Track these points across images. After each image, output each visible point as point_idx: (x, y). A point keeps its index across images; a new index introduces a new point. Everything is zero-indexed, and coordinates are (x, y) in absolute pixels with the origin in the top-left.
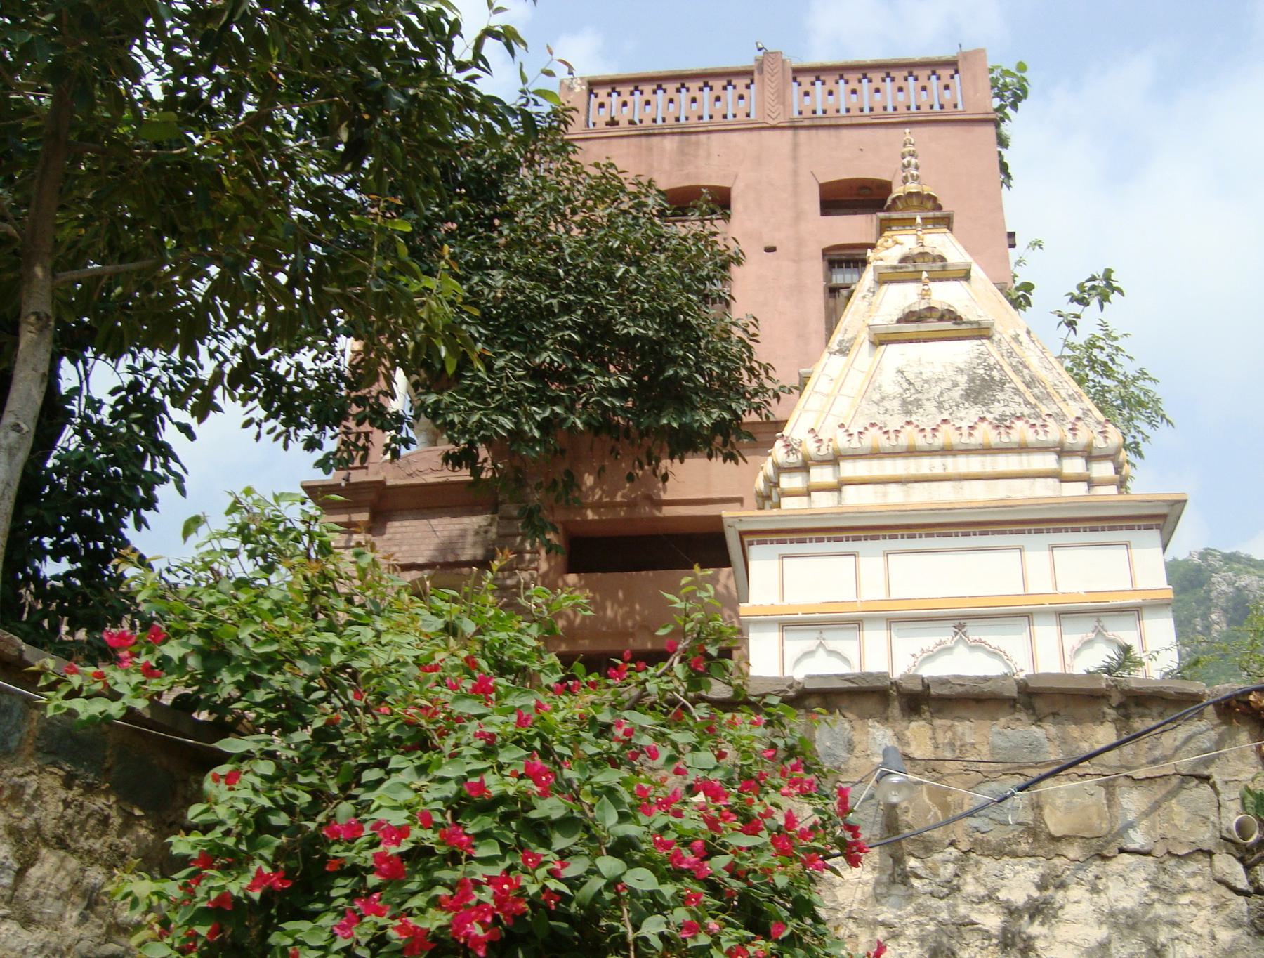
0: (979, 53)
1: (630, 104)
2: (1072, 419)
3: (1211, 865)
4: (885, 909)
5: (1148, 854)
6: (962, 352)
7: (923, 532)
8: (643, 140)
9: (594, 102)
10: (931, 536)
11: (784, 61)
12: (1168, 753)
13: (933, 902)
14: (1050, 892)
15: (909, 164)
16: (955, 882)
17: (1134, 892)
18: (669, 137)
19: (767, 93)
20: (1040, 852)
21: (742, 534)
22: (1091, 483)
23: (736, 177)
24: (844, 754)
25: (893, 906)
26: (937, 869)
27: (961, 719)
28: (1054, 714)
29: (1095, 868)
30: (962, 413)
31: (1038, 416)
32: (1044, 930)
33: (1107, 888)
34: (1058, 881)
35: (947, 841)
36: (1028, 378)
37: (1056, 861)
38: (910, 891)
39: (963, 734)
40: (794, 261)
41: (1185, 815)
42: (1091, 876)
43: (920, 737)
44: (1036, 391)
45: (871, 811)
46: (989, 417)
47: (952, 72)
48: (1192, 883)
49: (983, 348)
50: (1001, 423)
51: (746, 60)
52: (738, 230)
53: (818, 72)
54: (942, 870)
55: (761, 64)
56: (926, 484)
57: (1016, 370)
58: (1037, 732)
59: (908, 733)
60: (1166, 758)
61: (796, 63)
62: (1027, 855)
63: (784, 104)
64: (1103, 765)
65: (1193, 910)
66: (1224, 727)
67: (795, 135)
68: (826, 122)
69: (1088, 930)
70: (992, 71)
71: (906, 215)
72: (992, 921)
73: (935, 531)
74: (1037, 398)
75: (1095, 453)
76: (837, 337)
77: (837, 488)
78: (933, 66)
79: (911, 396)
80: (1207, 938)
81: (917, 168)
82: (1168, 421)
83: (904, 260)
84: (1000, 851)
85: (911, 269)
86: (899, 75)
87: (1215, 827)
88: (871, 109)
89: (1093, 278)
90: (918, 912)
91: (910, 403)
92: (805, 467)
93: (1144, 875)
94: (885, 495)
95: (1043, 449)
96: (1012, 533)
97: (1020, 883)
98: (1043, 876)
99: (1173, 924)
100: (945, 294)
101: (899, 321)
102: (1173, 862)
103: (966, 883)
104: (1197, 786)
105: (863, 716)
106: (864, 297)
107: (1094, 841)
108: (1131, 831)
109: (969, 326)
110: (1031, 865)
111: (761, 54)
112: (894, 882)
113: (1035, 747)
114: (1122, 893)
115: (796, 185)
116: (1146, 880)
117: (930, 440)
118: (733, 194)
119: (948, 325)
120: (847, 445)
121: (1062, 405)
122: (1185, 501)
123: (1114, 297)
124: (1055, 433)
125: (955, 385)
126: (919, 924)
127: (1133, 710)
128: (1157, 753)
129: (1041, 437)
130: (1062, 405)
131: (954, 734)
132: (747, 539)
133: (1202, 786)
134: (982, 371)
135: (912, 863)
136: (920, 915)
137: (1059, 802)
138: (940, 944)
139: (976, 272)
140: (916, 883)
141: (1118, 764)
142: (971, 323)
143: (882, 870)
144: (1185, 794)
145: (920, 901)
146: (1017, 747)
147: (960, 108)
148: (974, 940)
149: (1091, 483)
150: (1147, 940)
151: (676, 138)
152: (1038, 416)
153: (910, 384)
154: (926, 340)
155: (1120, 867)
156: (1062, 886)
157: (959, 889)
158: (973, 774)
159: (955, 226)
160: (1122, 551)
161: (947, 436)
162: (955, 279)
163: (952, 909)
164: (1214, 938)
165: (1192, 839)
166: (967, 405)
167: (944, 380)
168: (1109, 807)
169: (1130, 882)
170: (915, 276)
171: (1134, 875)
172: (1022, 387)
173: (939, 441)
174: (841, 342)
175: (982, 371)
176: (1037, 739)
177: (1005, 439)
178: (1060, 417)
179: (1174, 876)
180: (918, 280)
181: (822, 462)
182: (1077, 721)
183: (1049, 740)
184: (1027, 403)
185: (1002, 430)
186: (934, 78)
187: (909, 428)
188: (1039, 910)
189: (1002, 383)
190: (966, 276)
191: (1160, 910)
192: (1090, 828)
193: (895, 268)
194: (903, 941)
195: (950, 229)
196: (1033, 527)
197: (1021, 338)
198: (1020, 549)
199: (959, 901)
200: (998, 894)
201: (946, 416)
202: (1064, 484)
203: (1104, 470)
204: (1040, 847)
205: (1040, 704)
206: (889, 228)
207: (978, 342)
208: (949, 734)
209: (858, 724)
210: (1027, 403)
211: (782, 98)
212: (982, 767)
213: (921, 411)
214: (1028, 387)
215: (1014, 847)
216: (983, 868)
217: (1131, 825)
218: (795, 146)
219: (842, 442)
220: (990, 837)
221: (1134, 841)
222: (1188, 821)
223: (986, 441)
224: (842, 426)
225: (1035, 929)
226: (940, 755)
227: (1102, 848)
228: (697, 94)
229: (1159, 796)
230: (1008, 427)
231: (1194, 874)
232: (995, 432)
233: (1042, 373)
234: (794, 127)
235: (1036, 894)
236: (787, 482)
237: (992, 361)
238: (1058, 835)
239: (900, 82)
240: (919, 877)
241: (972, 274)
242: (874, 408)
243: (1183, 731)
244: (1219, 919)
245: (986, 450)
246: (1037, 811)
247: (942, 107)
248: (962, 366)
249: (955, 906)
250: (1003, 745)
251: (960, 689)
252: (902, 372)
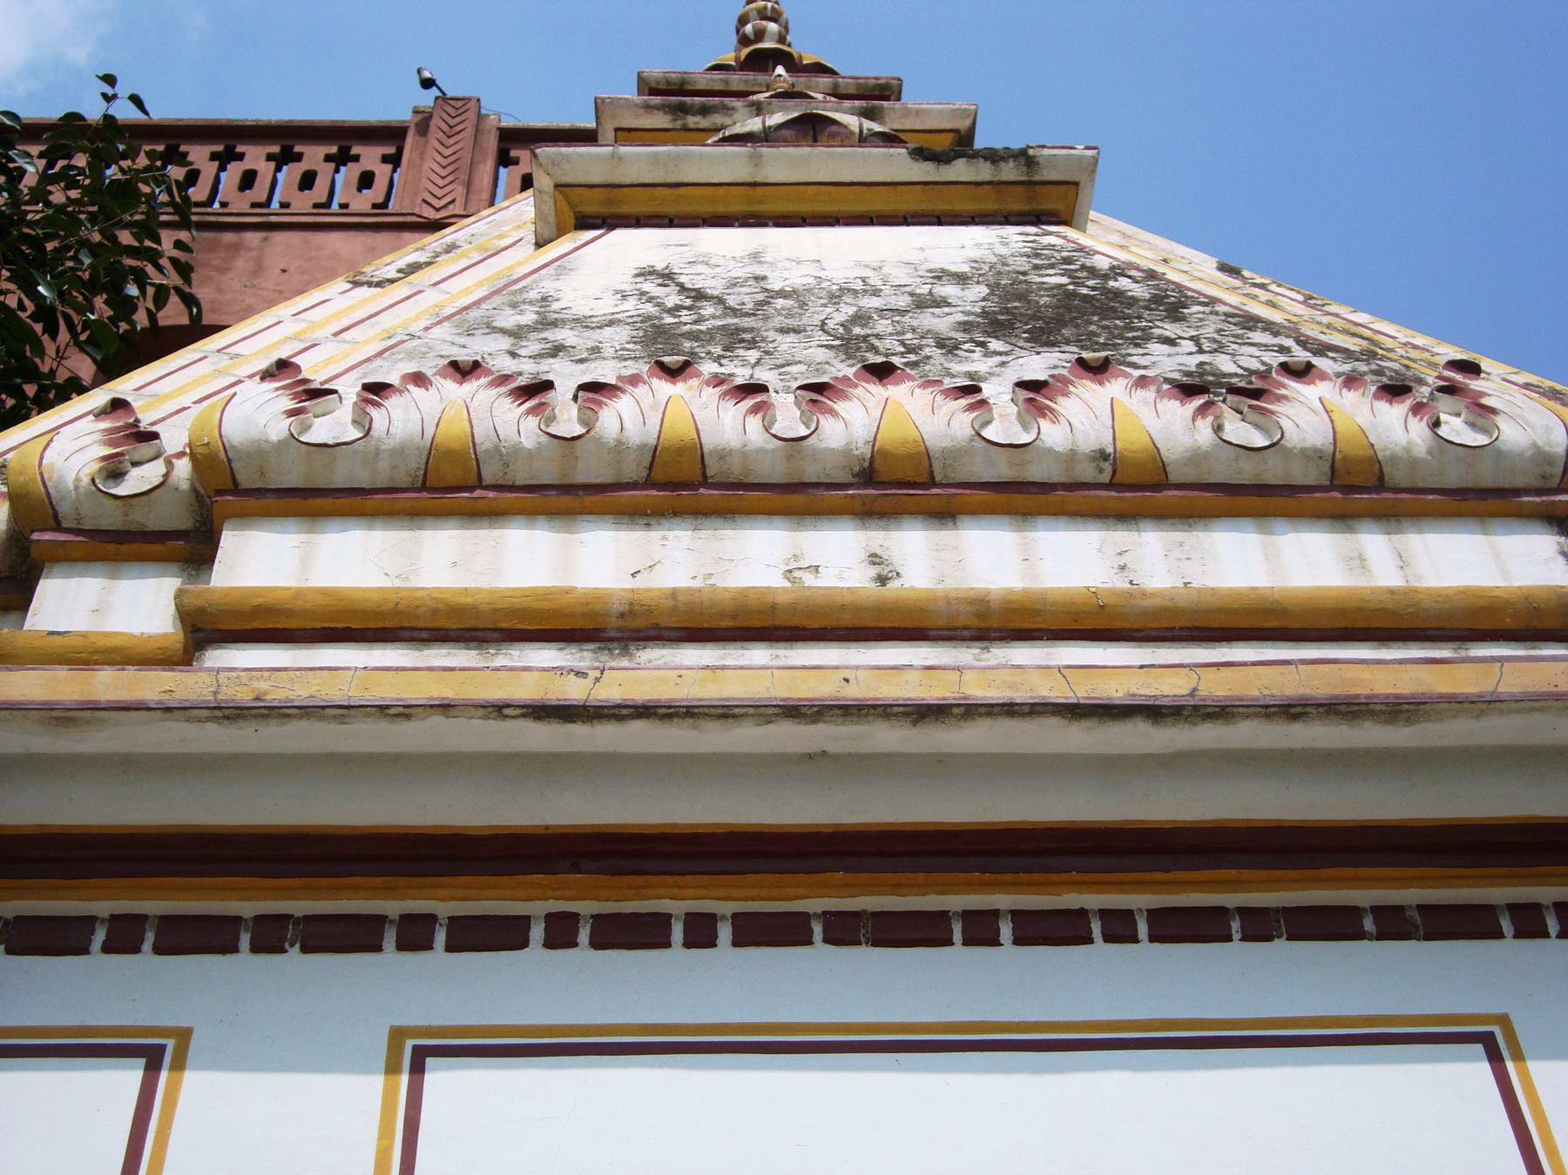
51: (396, 103)
55: (424, 121)
61: (507, 123)
109: (984, 172)
111: (427, 98)
198: (1493, 1044)
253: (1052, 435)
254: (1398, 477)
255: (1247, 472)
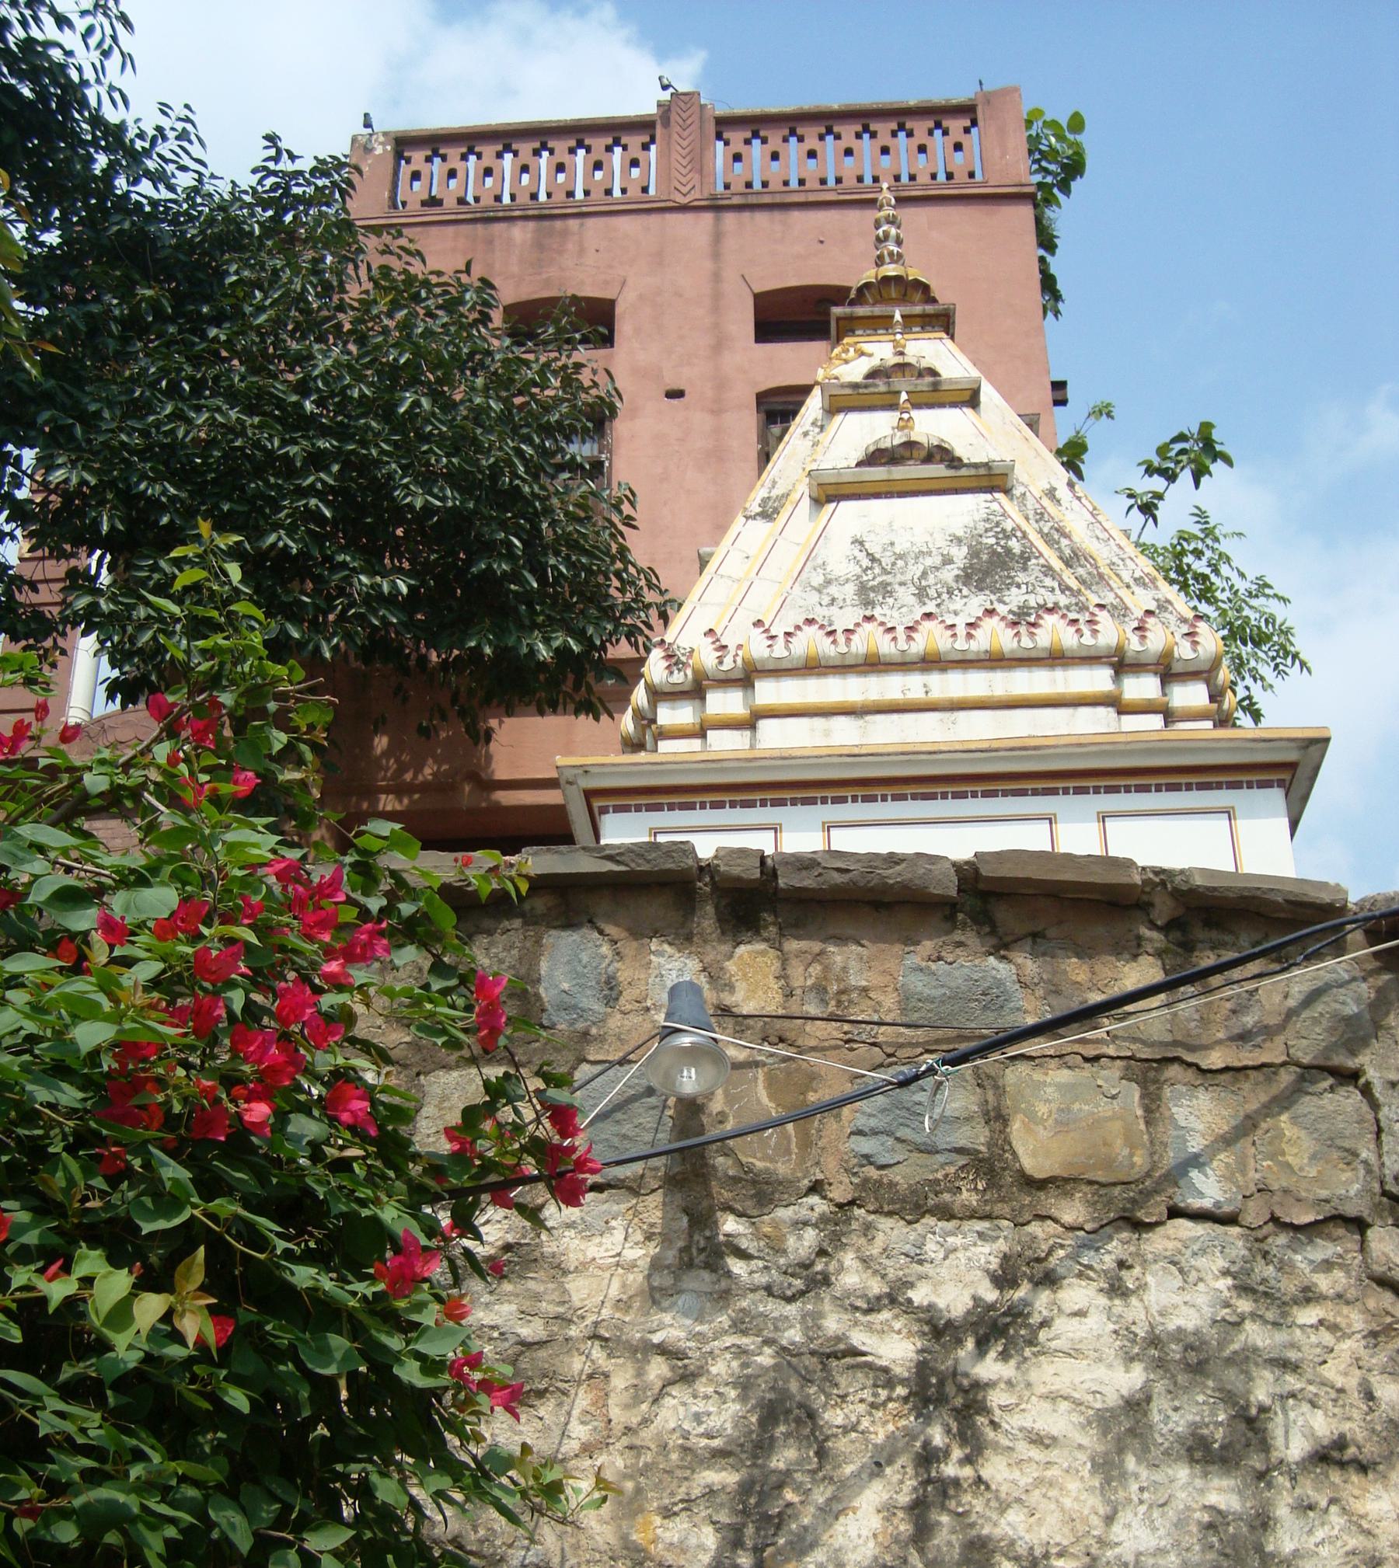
0: (1010, 93)
1: (460, 174)
2: (1139, 614)
3: (1363, 1248)
4: (667, 1318)
5: (1230, 1220)
6: (964, 511)
7: (889, 791)
8: (479, 227)
9: (405, 170)
10: (901, 797)
11: (703, 107)
12: (1273, 1021)
13: (773, 1308)
14: (1022, 1292)
15: (887, 235)
16: (819, 1267)
17: (1201, 1297)
18: (520, 224)
19: (675, 156)
20: (999, 1209)
21: (590, 794)
22: (1169, 716)
23: (624, 283)
24: (598, 1007)
25: (686, 1315)
26: (782, 1238)
27: (841, 940)
28: (1035, 936)
29: (1116, 1247)
30: (957, 603)
31: (1083, 608)
32: (1007, 1370)
33: (1143, 1287)
34: (1038, 1270)
35: (806, 1183)
36: (1067, 552)
37: (1035, 1228)
38: (724, 1284)
39: (845, 969)
40: (712, 412)
41: (1308, 1144)
42: (1109, 1262)
43: (754, 974)
44: (1081, 571)
45: (648, 1119)
46: (1002, 609)
47: (968, 123)
48: (1324, 1283)
49: (995, 506)
50: (1020, 619)
52: (628, 365)
53: (756, 125)
54: (791, 1242)
56: (895, 717)
57: (1047, 539)
58: (999, 969)
59: (731, 966)
60: (1268, 1032)
61: (721, 111)
62: (974, 1215)
63: (701, 172)
64: (1135, 1040)
65: (1327, 1338)
66: (1387, 977)
67: (717, 220)
68: (767, 199)
69: (1101, 1372)
70: (1029, 123)
71: (878, 310)
72: (896, 1348)
73: (909, 790)
74: (1083, 582)
75: (1177, 668)
76: (760, 493)
77: (749, 723)
78: (937, 114)
79: (874, 578)
80: (1355, 1397)
81: (899, 242)
82: (1303, 664)
83: (873, 374)
84: (915, 1206)
85: (882, 388)
86: (883, 128)
87: (1369, 1171)
88: (839, 180)
89: (1181, 438)
90: (739, 1326)
91: (873, 589)
92: (696, 691)
93: (1221, 1263)
94: (827, 733)
95: (1090, 659)
96: (1035, 792)
97: (957, 1271)
98: (1006, 1258)
99: (1285, 1365)
100: (933, 425)
101: (859, 464)
102: (1282, 1239)
103: (841, 1269)
104: (1332, 1089)
105: (640, 932)
106: (806, 434)
107: (1117, 1191)
108: (1194, 1174)
109: (973, 472)
110: (980, 1235)
111: (666, 96)
112: (690, 1265)
113: (993, 998)
114: (1177, 1299)
115: (717, 297)
116: (1226, 1273)
117: (902, 645)
118: (619, 310)
119: (938, 470)
120: (766, 653)
121: (1124, 593)
122: (1327, 740)
123: (1217, 467)
124: (1109, 633)
125: (948, 561)
126: (741, 1352)
127: (1199, 933)
128: (1249, 1020)
129: (1088, 640)
130: (1124, 593)
131: (826, 969)
132: (597, 804)
133: (1342, 1091)
134: (993, 541)
135: (730, 1225)
136: (744, 1333)
137: (1042, 1109)
138: (784, 1395)
139: (989, 394)
140: (737, 1266)
141: (1168, 1038)
142: (976, 466)
143: (666, 1239)
144: (1307, 1105)
145: (744, 1304)
146: (955, 997)
147: (979, 177)
148: (856, 1387)
149: (1169, 716)
150: (1228, 1397)
151: (531, 225)
152: (1083, 608)
153: (873, 559)
154: (902, 494)
155: (1170, 1245)
156: (1050, 1280)
157: (826, 1281)
158: (863, 1049)
159: (959, 328)
160: (1222, 822)
161: (932, 638)
162: (954, 405)
163: (811, 1321)
164: (1369, 1396)
165: (1324, 1193)
166: (965, 591)
167: (930, 553)
168: (1147, 1123)
169: (1193, 1276)
170: (888, 399)
171: (1201, 1262)
172: (1057, 564)
173: (918, 646)
174: (765, 501)
175: (993, 541)
176: (999, 983)
177: (1026, 642)
178: (1120, 611)
179: (1284, 1267)
180: (892, 406)
181: (726, 682)
182: (1084, 952)
183: (1024, 985)
184: (1065, 588)
185: (1023, 629)
186: (938, 133)
187: (868, 627)
188: (1000, 1328)
189: (1024, 559)
190: (971, 399)
191: (1255, 1334)
192: (1108, 1163)
193: (855, 386)
194: (703, 1387)
195: (952, 338)
196: (1071, 784)
197: (1058, 494)
199: (827, 1306)
200: (910, 1294)
201: (931, 607)
202: (1124, 718)
203: (1191, 695)
204: (1002, 1200)
205: (1003, 914)
206: (851, 332)
207: (988, 496)
208: (816, 969)
209: (629, 947)
210: (1065, 588)
211: (699, 163)
212: (884, 1034)
213: (890, 601)
214: (1068, 564)
215: (946, 1197)
216: (880, 1239)
217: (1197, 1161)
218: (718, 237)
219: (759, 649)
220: (896, 1175)
221: (1201, 1195)
222: (1313, 1157)
223: (995, 647)
224: (758, 623)
225: (989, 1368)
226: (795, 1010)
227: (1134, 1206)
228: (566, 158)
229: (1253, 1106)
230: (1033, 625)
231: (1327, 1266)
232: (1011, 632)
233: (1090, 546)
234: (715, 207)
235: (990, 1294)
236: (669, 715)
237: (1008, 525)
238: (1039, 1175)
239: (884, 138)
240: (743, 1255)
241: (983, 398)
242: (814, 597)
243: (1301, 978)
244: (1381, 1358)
245: (995, 661)
246: (998, 1126)
247: (950, 176)
248: (960, 533)
249: (818, 1315)
250: (927, 991)
251: (839, 879)
252: (861, 543)
253: (974, 646)
254: (1068, 654)
255: (1026, 655)
